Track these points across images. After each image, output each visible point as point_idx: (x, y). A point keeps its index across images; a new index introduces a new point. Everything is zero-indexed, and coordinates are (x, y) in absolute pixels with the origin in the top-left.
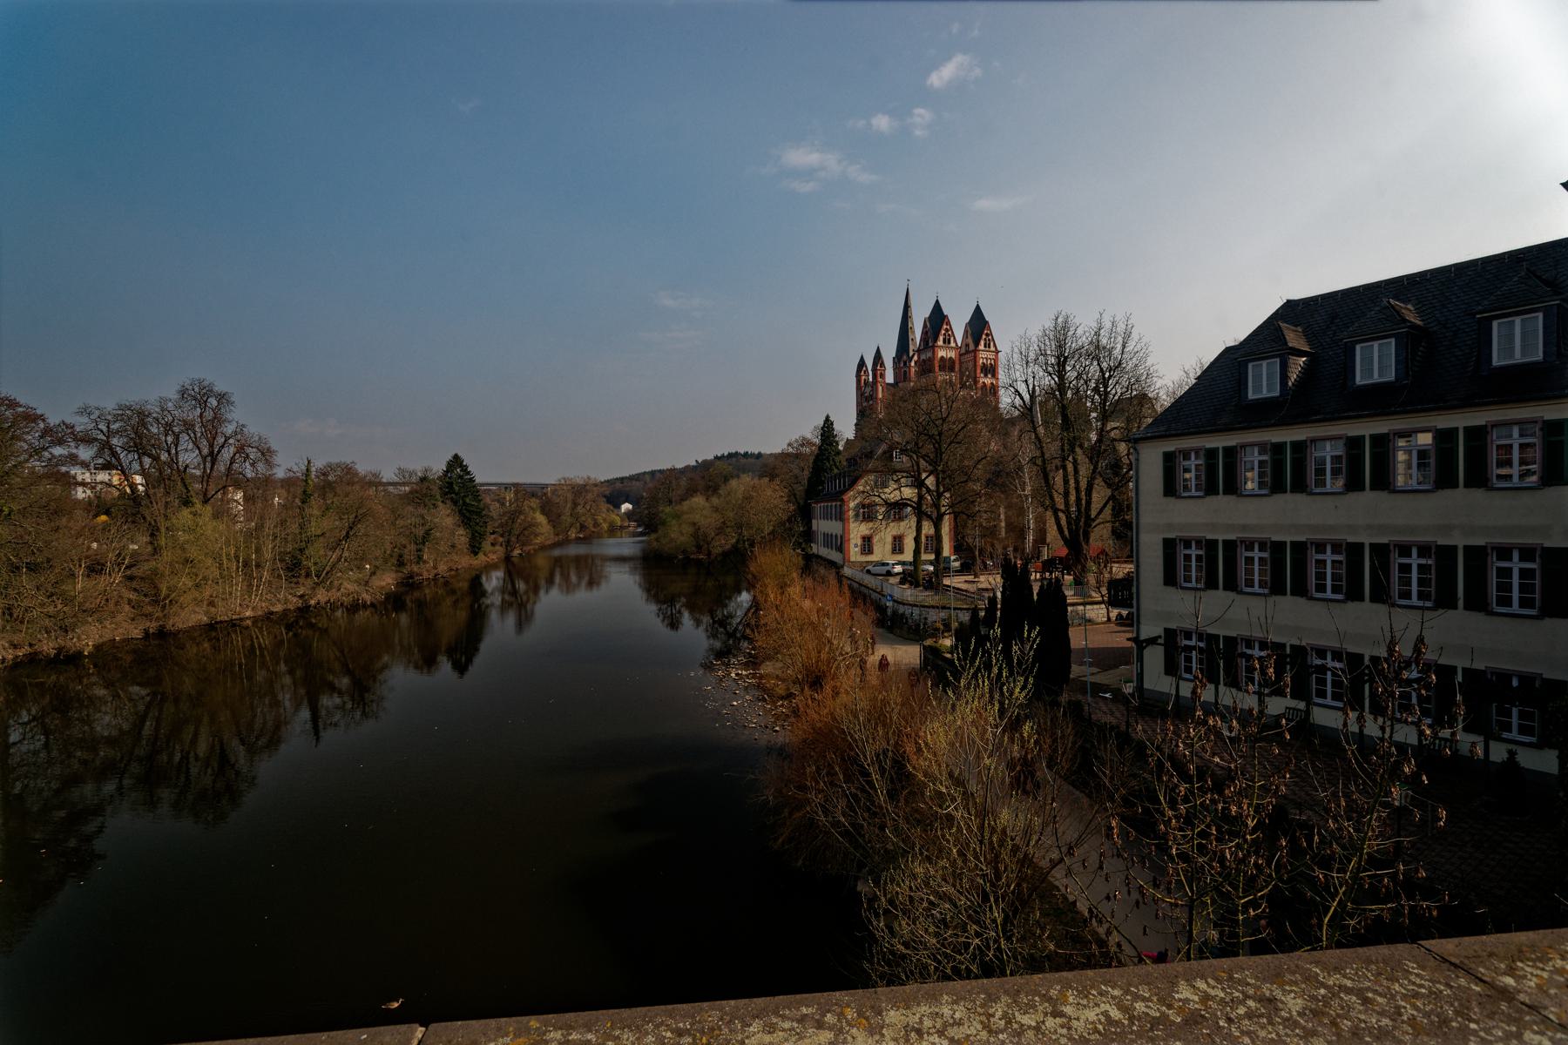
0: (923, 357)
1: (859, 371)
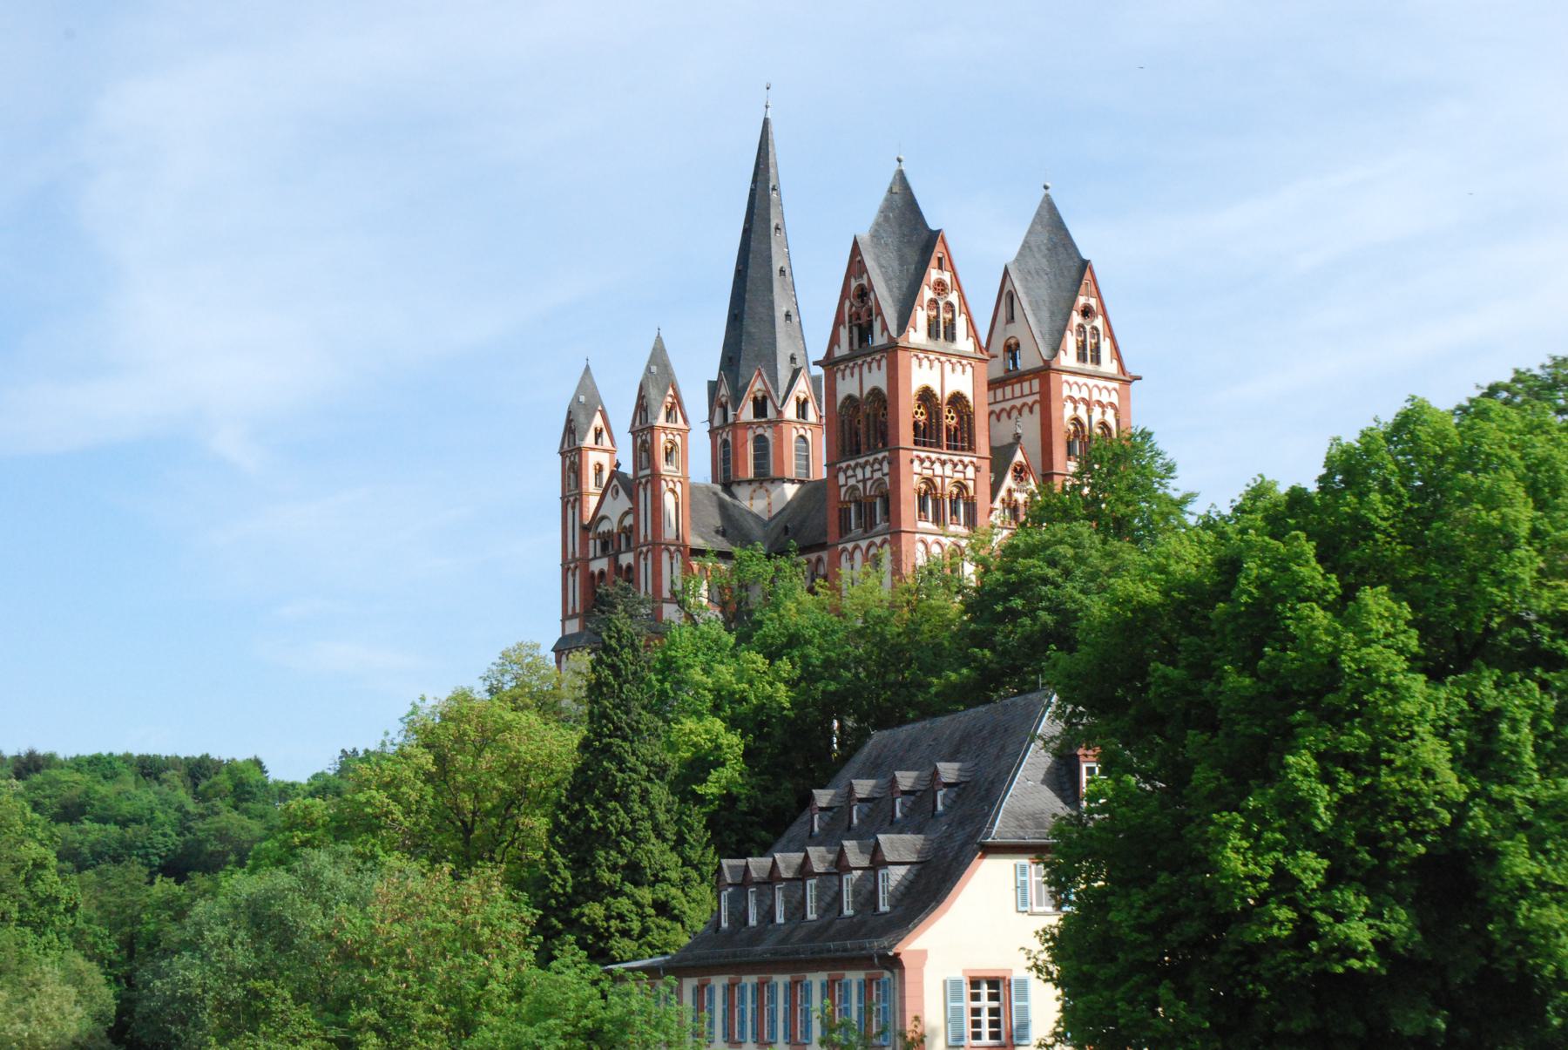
0: (848, 386)
1: (571, 430)
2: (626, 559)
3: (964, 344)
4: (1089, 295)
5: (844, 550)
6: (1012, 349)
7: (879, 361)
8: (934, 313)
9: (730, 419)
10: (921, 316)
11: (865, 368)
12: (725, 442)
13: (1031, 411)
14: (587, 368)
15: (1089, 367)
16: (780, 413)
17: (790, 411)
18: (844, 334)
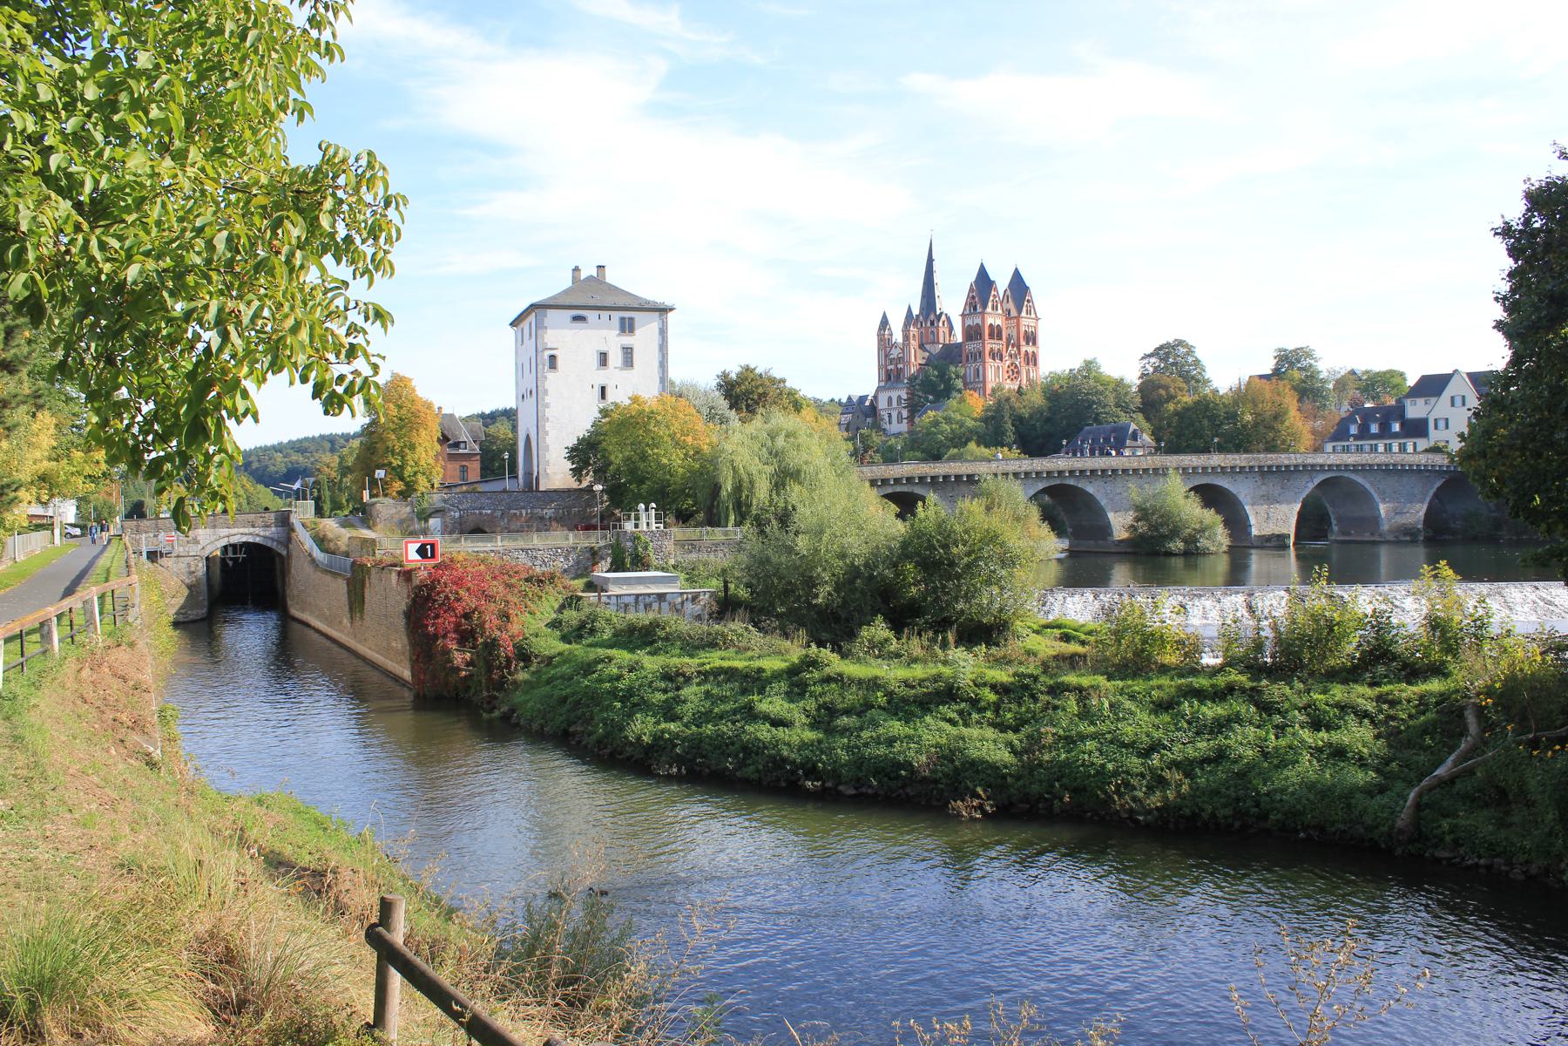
0: (969, 322)
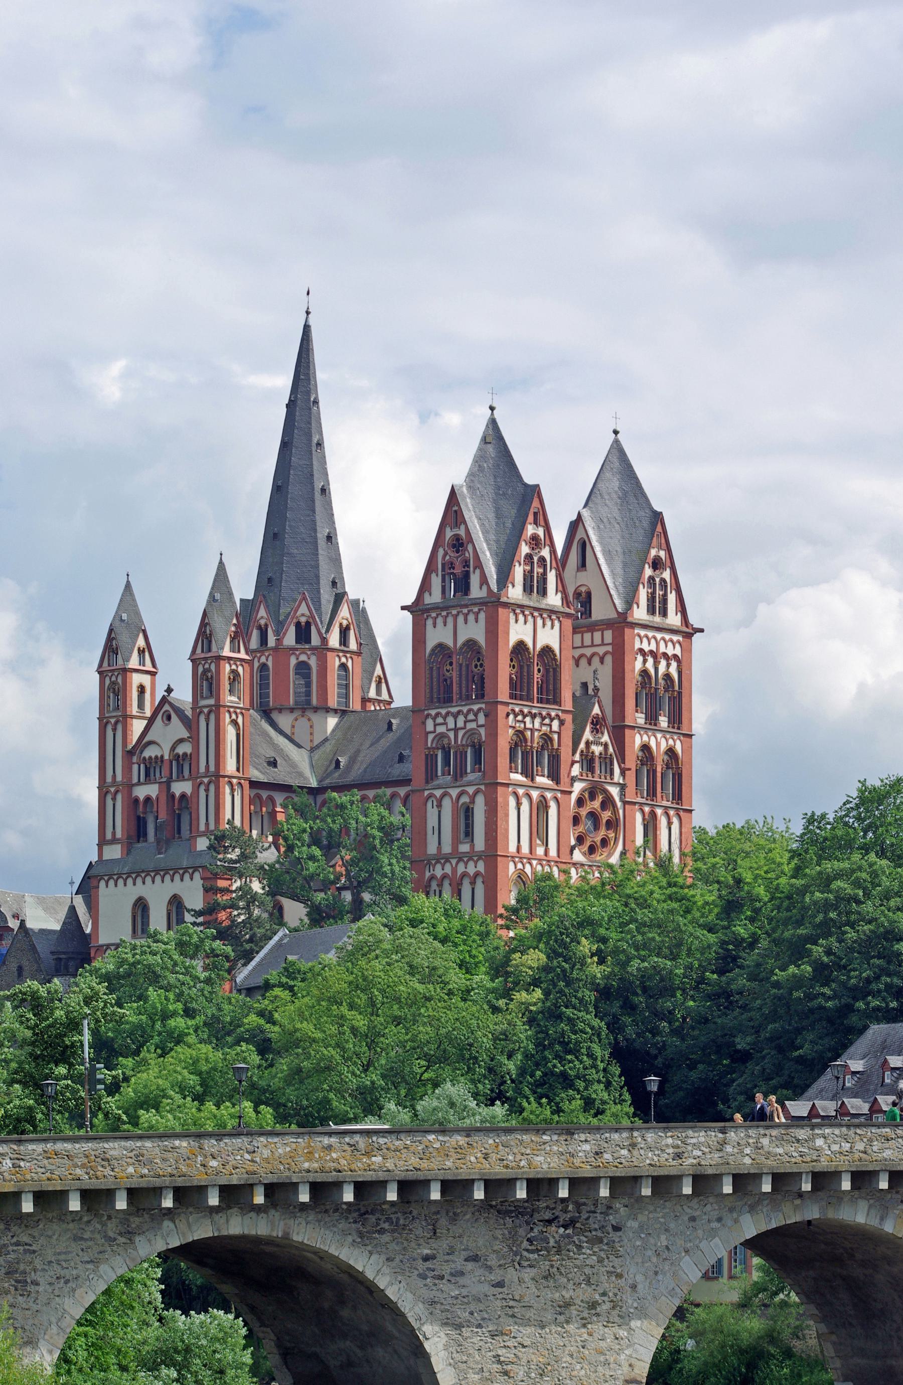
0: (439, 634)
2: (181, 788)
3: (554, 599)
4: (660, 548)
5: (431, 796)
6: (585, 600)
7: (477, 614)
8: (528, 568)
9: (272, 641)
10: (519, 572)
11: (461, 619)
12: (264, 667)
13: (602, 661)
14: (128, 586)
15: (657, 619)
16: (324, 640)
17: (334, 640)
18: (436, 582)
